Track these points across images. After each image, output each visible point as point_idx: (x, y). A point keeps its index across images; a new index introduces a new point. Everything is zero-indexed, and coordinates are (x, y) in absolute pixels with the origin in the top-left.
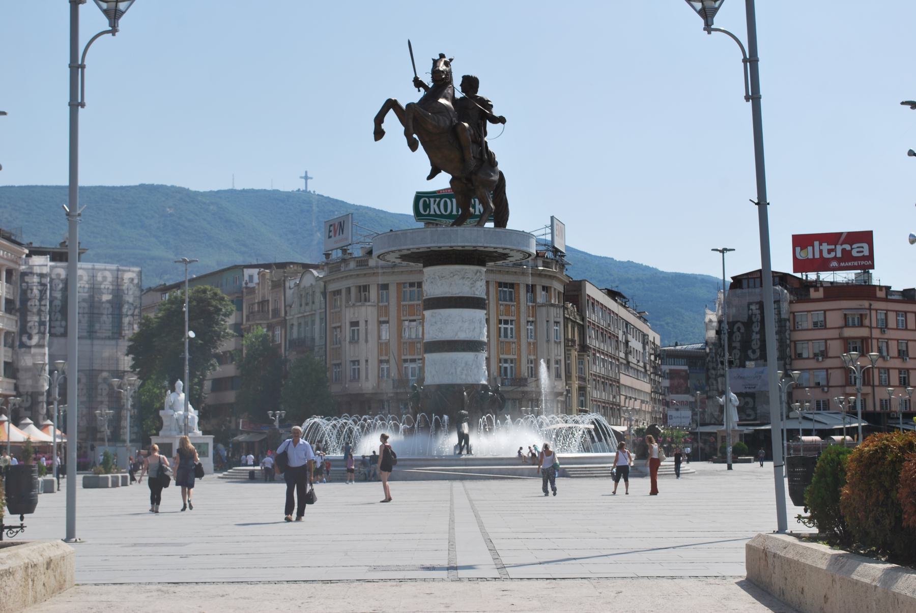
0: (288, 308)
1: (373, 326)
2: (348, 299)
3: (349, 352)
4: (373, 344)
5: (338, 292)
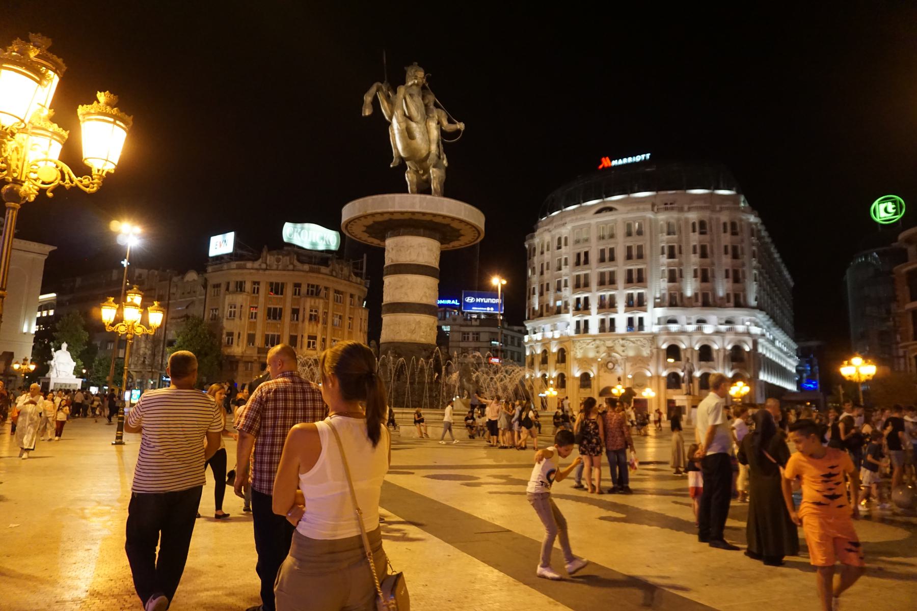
0: (172, 296)
1: (246, 310)
2: (227, 289)
3: (228, 325)
4: (245, 321)
5: (217, 286)
